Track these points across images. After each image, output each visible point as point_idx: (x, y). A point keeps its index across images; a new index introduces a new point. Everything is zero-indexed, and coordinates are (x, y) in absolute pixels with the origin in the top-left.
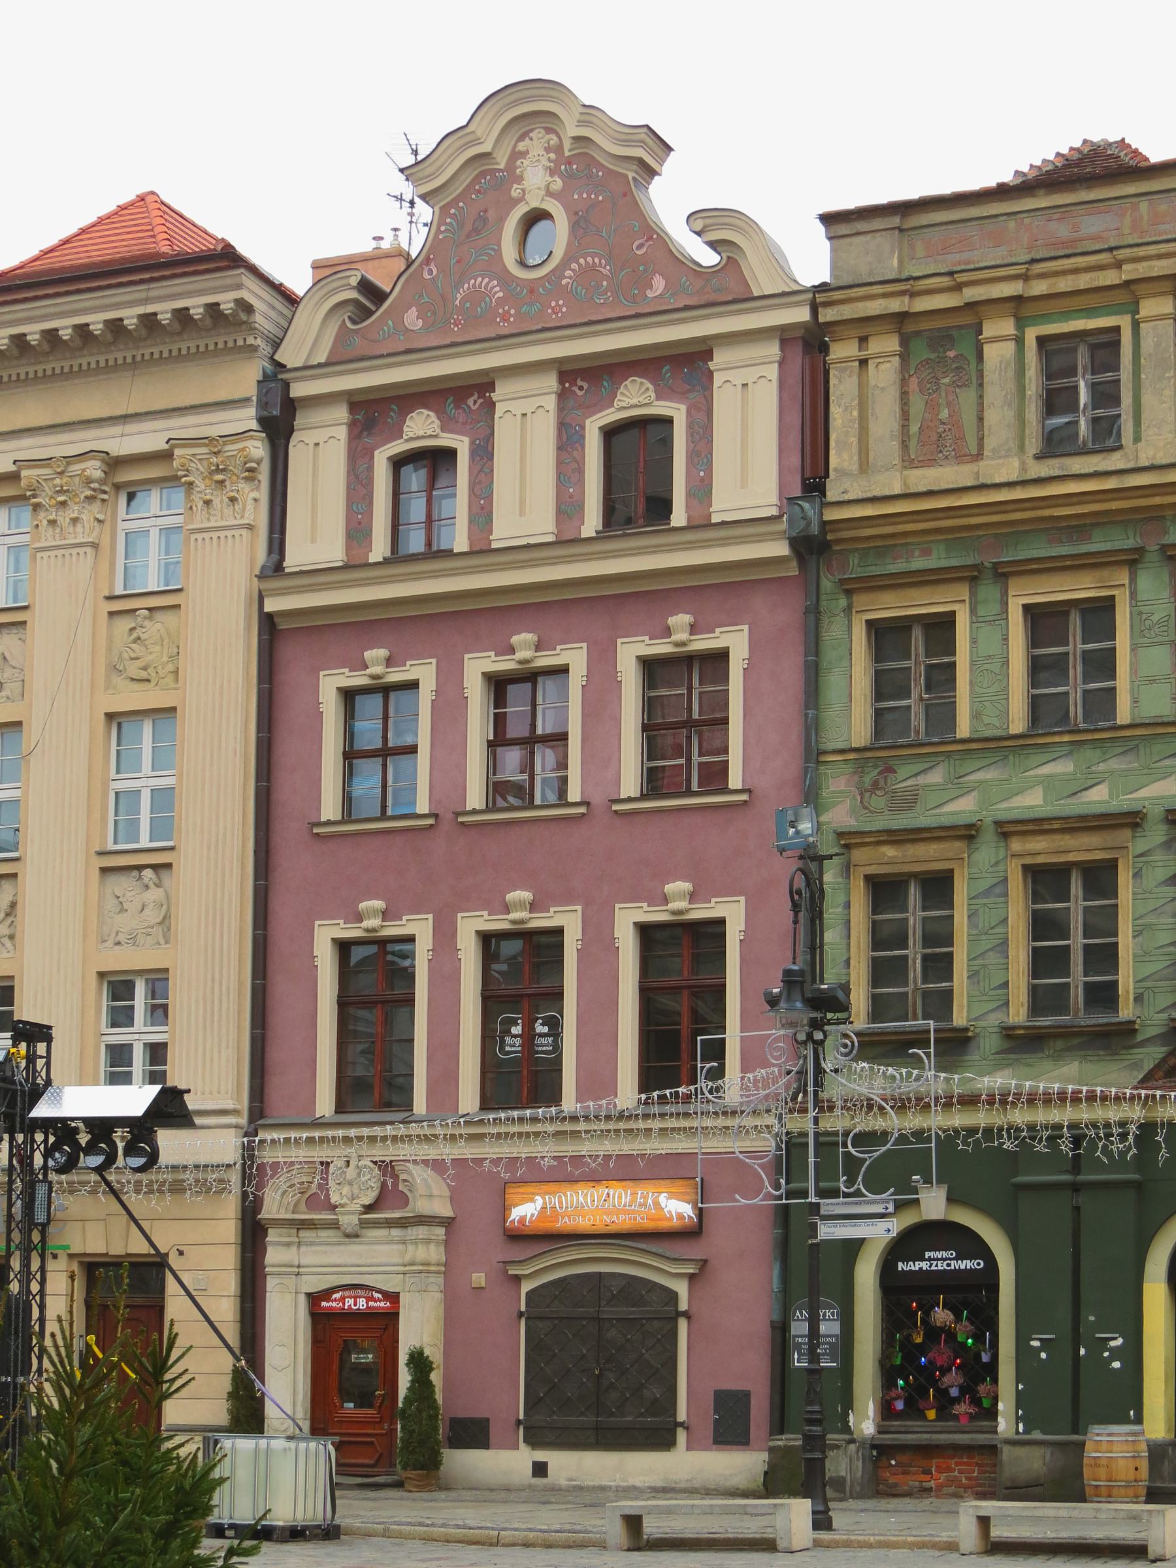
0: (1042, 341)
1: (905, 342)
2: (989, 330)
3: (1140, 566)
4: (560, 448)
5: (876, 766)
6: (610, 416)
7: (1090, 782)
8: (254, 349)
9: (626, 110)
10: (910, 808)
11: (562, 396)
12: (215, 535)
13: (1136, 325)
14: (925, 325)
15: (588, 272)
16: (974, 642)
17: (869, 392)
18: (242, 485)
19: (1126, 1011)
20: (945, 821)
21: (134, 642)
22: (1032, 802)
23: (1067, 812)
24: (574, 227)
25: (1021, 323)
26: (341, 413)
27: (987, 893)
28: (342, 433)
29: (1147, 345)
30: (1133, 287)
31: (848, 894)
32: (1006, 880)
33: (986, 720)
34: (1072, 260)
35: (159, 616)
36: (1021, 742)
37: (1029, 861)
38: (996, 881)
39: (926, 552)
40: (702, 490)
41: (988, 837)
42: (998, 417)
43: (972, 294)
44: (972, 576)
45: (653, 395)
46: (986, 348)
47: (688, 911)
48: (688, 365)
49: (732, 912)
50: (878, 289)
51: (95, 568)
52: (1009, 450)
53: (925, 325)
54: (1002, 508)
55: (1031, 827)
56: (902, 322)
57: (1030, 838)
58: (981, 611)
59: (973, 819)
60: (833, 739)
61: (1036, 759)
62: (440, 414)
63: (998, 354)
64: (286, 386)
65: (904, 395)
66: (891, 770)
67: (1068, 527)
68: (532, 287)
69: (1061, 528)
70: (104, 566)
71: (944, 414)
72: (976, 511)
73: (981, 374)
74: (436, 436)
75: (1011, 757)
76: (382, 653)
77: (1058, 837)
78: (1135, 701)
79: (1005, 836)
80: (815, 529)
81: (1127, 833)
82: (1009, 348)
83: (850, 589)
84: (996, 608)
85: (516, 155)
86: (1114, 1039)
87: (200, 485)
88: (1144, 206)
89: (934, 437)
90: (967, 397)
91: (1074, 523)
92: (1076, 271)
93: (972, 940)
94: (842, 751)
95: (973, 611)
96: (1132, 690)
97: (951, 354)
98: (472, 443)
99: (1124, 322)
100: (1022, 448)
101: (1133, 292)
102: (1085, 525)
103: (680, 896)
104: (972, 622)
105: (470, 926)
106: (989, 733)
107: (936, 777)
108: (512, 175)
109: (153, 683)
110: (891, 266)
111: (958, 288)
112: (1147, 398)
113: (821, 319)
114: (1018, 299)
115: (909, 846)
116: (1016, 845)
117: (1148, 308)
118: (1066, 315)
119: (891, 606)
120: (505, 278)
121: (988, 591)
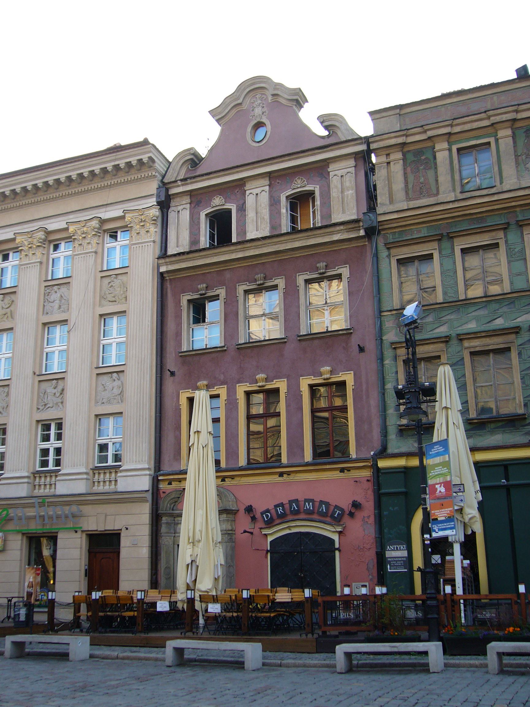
0: (459, 150)
1: (404, 155)
2: (438, 147)
3: (508, 230)
6: (290, 192)
9: (291, 84)
12: (141, 245)
13: (497, 140)
14: (412, 148)
16: (441, 265)
20: (434, 336)
21: (110, 287)
22: (472, 326)
23: (487, 329)
26: (187, 199)
30: (495, 126)
31: (397, 368)
33: (449, 295)
34: (470, 117)
35: (120, 277)
36: (465, 302)
37: (472, 350)
38: (459, 359)
39: (419, 231)
41: (454, 342)
42: (444, 178)
43: (430, 133)
44: (439, 238)
45: (305, 182)
46: (437, 154)
47: (330, 378)
49: (349, 378)
52: (450, 191)
53: (412, 148)
56: (403, 147)
57: (472, 341)
58: (443, 253)
59: (448, 334)
60: (386, 306)
63: (442, 157)
65: (405, 174)
67: (477, 218)
69: (473, 219)
70: (99, 261)
71: (422, 180)
72: (439, 213)
73: (436, 164)
75: (461, 309)
77: (484, 339)
78: (511, 283)
80: (375, 224)
81: (513, 336)
82: (447, 153)
83: (389, 247)
84: (449, 251)
88: (495, 98)
89: (418, 189)
90: (431, 174)
91: (479, 216)
94: (390, 311)
96: (510, 278)
97: (423, 158)
98: (237, 206)
100: (454, 190)
101: (495, 128)
102: (483, 217)
104: (440, 257)
106: (451, 300)
109: (117, 302)
111: (425, 132)
112: (504, 167)
113: (371, 148)
114: (450, 134)
116: (466, 344)
117: (501, 133)
118: (468, 139)
121: (446, 244)
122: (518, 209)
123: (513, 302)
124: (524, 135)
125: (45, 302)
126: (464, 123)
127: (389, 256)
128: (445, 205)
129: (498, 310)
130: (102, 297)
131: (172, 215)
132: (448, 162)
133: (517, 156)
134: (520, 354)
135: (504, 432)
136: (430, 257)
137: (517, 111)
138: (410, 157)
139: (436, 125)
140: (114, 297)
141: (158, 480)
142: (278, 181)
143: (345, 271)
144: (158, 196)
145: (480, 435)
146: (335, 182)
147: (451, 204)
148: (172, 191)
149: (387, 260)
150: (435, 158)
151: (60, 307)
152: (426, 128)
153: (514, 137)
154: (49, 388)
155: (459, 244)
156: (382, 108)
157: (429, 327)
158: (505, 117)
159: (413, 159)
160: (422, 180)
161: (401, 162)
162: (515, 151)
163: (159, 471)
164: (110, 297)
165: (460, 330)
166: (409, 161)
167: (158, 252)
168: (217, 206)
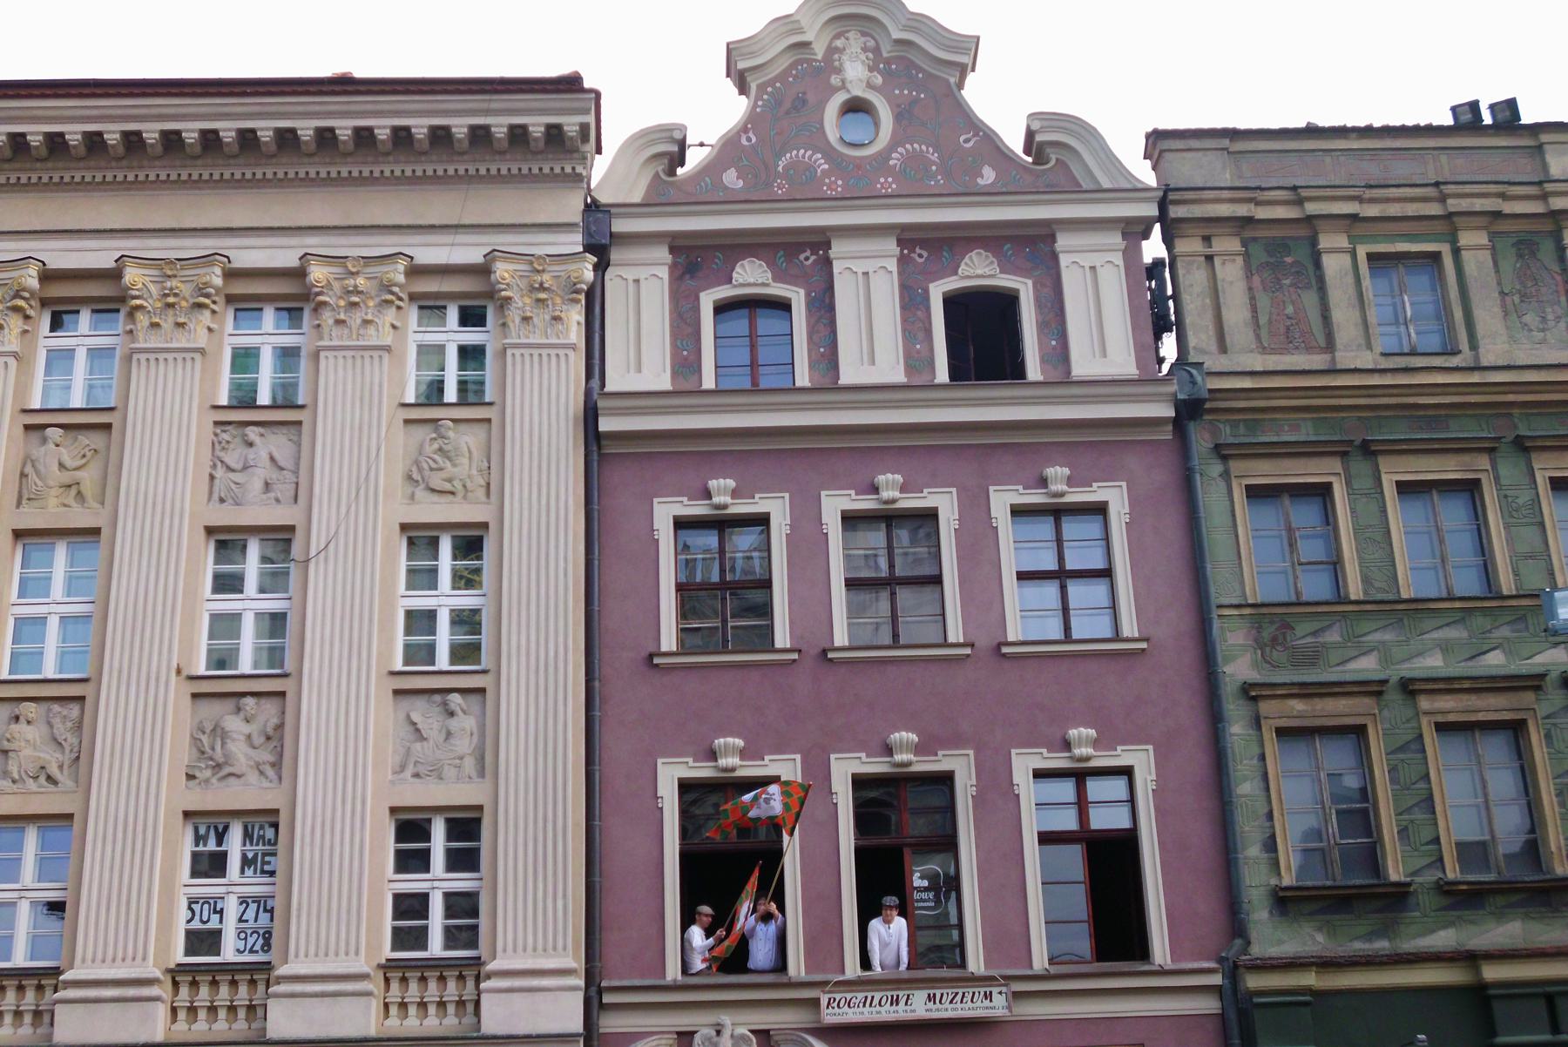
0: (1371, 257)
2: (1325, 242)
4: (903, 308)
5: (1272, 623)
7: (1486, 648)
9: (956, 21)
10: (1313, 664)
11: (903, 261)
13: (1456, 252)
15: (913, 159)
20: (1348, 677)
22: (1433, 663)
24: (898, 117)
26: (662, 254)
27: (1402, 748)
28: (664, 273)
30: (1455, 219)
32: (1421, 736)
33: (1377, 584)
34: (1401, 190)
37: (1440, 719)
38: (1410, 737)
39: (1295, 428)
40: (1059, 354)
42: (1344, 315)
43: (1312, 208)
44: (1341, 451)
48: (1034, 245)
50: (1226, 194)
54: (1371, 392)
55: (1442, 686)
57: (1438, 697)
61: (1428, 624)
62: (771, 265)
63: (1334, 266)
68: (859, 164)
71: (1290, 310)
74: (767, 285)
76: (731, 483)
77: (1465, 697)
82: (1347, 259)
85: (831, 51)
87: (518, 301)
88: (1444, 158)
89: (1282, 330)
95: (1348, 483)
97: (1289, 260)
98: (808, 295)
105: (844, 769)
106: (1379, 597)
107: (1333, 636)
108: (830, 65)
110: (1226, 179)
112: (1479, 314)
114: (1354, 218)
115: (1317, 700)
116: (1424, 703)
117: (1465, 239)
120: (829, 153)
121: (1360, 466)
122: (1516, 411)
123: (1523, 618)
124: (1513, 250)
125: (214, 466)
126: (1388, 200)
128: (1364, 375)
129: (1490, 631)
132: (1350, 279)
134: (1548, 736)
135: (1527, 917)
137: (1503, 196)
139: (1329, 192)
140: (450, 480)
141: (602, 1006)
142: (918, 250)
145: (1472, 922)
147: (1376, 375)
149: (1222, 484)
150: (1318, 265)
151: (267, 485)
152: (1304, 193)
155: (1393, 471)
156: (1193, 126)
157: (1334, 657)
158: (1479, 205)
159: (1264, 258)
160: (1290, 310)
161: (1240, 260)
164: (437, 481)
166: (1255, 264)
168: (749, 285)
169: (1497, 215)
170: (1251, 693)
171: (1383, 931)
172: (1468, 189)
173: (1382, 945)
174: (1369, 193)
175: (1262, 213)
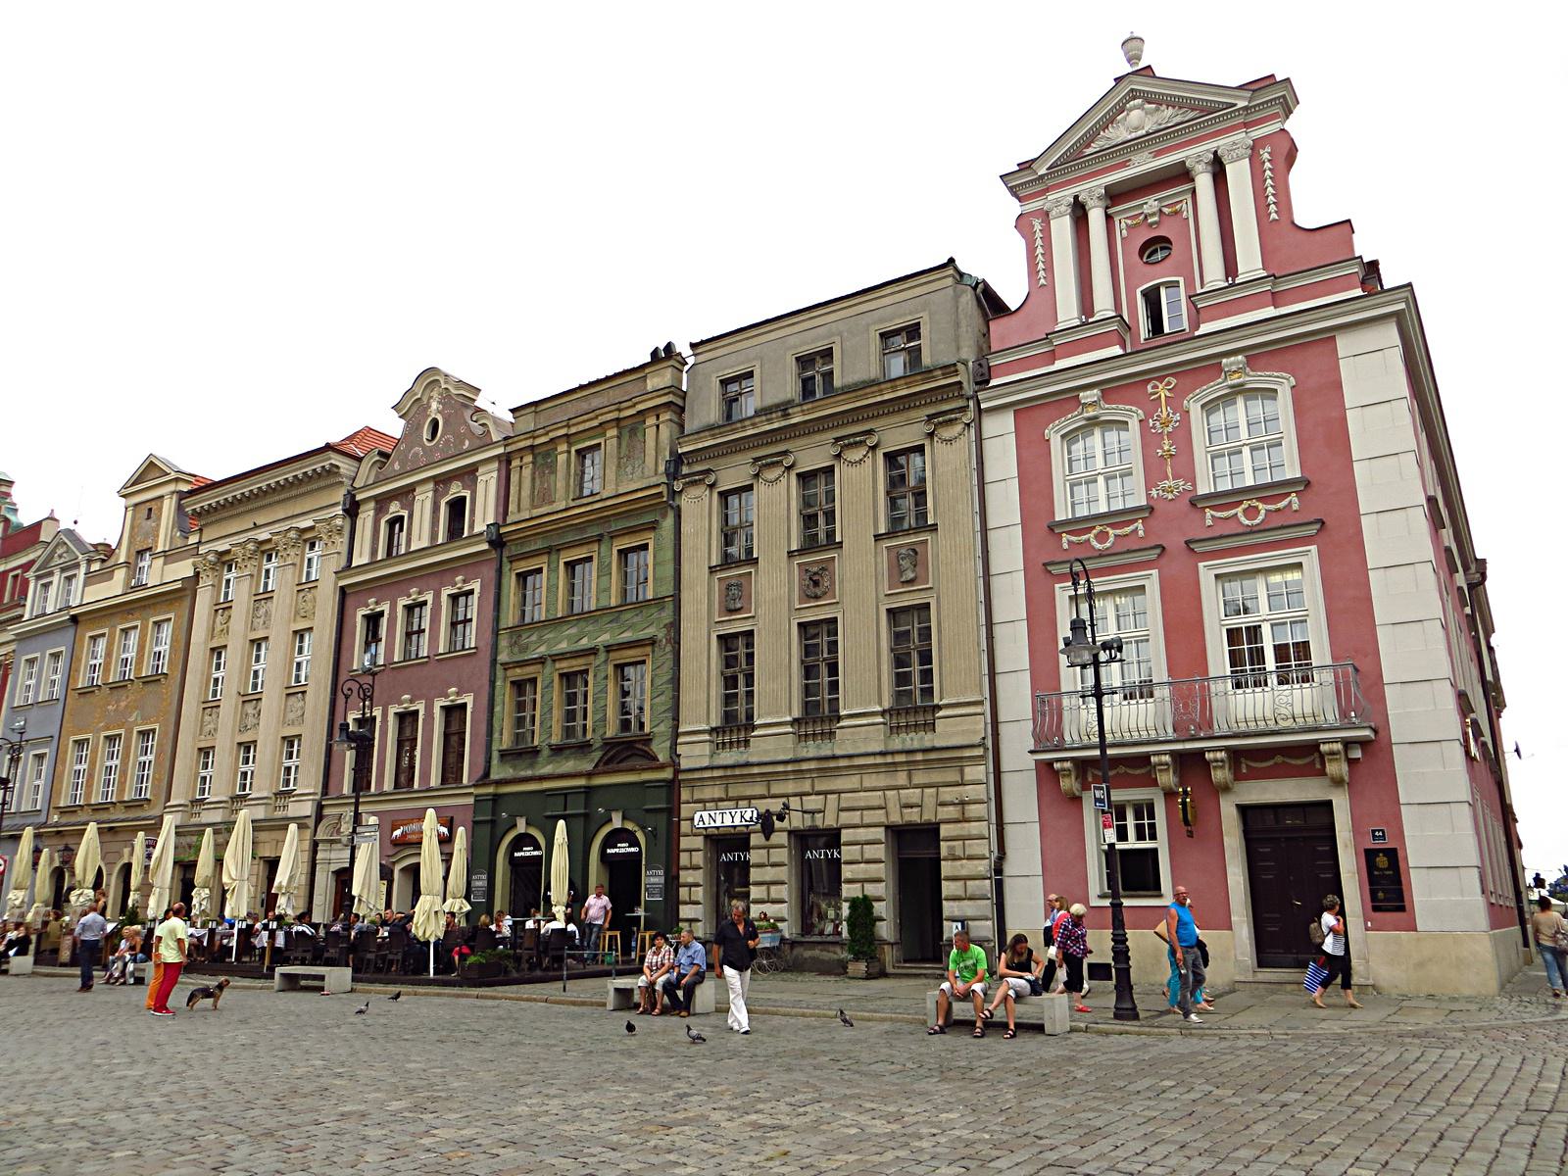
1: (534, 458)
8: (342, 483)
11: (435, 491)
16: (548, 579)
17: (523, 474)
18: (337, 537)
19: (589, 737)
22: (563, 646)
25: (570, 445)
27: (547, 687)
29: (608, 448)
41: (549, 662)
42: (560, 484)
43: (552, 435)
44: (548, 551)
49: (468, 699)
50: (522, 437)
51: (294, 573)
60: (503, 625)
63: (562, 458)
64: (354, 496)
65: (533, 479)
66: (520, 636)
76: (373, 599)
78: (598, 600)
79: (554, 661)
81: (592, 657)
86: (584, 747)
90: (553, 477)
92: (584, 422)
93: (542, 707)
99: (601, 440)
103: (452, 694)
107: (534, 638)
114: (566, 435)
116: (558, 665)
118: (584, 440)
119: (524, 566)
121: (554, 557)
127: (510, 570)
130: (297, 613)
131: (359, 522)
133: (620, 458)
135: (575, 759)
136: (539, 571)
138: (540, 460)
143: (476, 586)
144: (344, 504)
146: (480, 487)
148: (359, 497)
153: (619, 437)
154: (250, 709)
162: (619, 453)
163: (326, 794)
165: (556, 650)
167: (343, 562)
169: (618, 420)
170: (506, 666)
171: (532, 766)
172: (606, 410)
173: (529, 773)
174: (572, 422)
175: (538, 441)
